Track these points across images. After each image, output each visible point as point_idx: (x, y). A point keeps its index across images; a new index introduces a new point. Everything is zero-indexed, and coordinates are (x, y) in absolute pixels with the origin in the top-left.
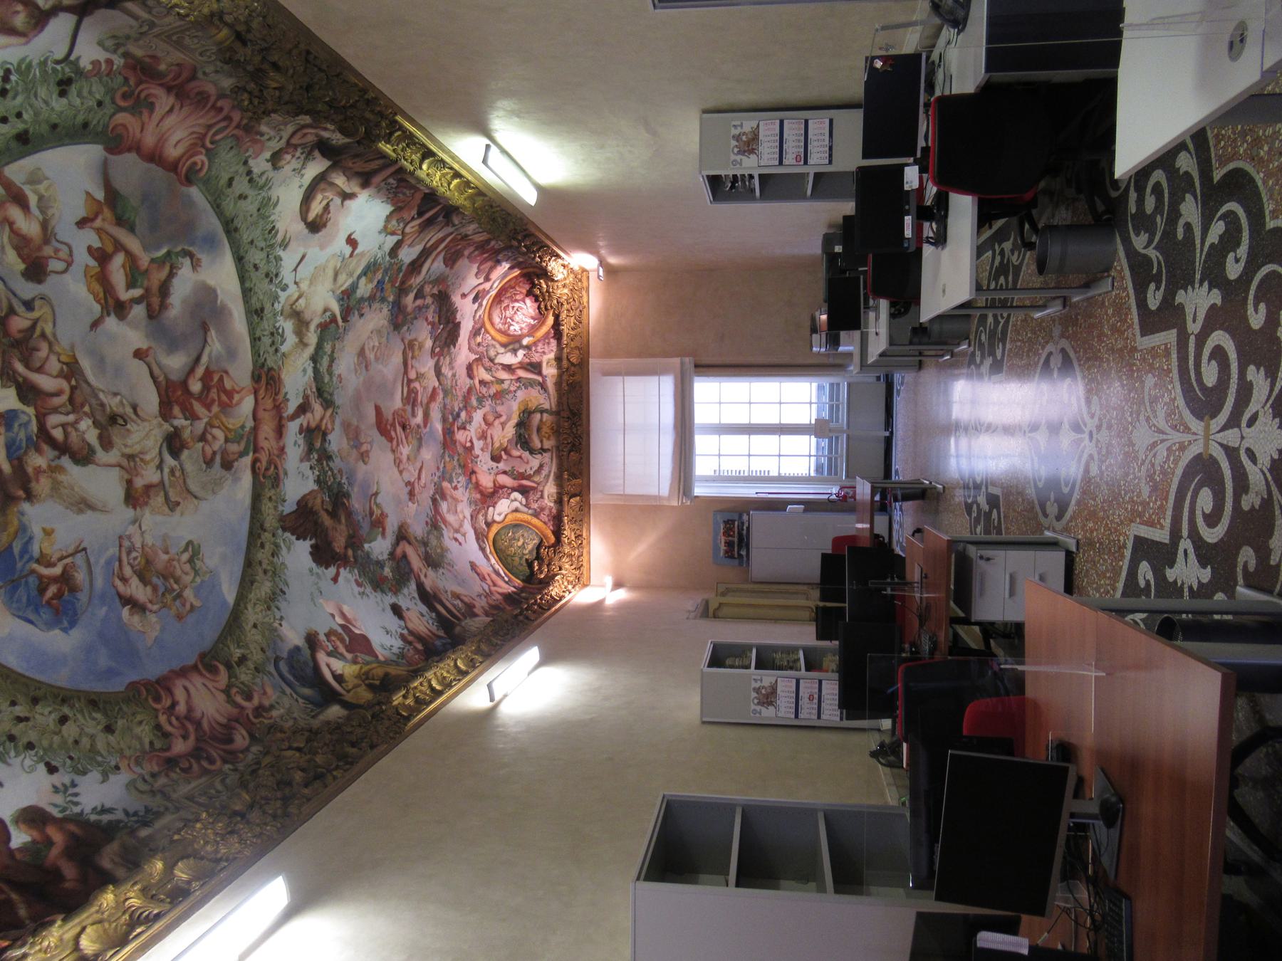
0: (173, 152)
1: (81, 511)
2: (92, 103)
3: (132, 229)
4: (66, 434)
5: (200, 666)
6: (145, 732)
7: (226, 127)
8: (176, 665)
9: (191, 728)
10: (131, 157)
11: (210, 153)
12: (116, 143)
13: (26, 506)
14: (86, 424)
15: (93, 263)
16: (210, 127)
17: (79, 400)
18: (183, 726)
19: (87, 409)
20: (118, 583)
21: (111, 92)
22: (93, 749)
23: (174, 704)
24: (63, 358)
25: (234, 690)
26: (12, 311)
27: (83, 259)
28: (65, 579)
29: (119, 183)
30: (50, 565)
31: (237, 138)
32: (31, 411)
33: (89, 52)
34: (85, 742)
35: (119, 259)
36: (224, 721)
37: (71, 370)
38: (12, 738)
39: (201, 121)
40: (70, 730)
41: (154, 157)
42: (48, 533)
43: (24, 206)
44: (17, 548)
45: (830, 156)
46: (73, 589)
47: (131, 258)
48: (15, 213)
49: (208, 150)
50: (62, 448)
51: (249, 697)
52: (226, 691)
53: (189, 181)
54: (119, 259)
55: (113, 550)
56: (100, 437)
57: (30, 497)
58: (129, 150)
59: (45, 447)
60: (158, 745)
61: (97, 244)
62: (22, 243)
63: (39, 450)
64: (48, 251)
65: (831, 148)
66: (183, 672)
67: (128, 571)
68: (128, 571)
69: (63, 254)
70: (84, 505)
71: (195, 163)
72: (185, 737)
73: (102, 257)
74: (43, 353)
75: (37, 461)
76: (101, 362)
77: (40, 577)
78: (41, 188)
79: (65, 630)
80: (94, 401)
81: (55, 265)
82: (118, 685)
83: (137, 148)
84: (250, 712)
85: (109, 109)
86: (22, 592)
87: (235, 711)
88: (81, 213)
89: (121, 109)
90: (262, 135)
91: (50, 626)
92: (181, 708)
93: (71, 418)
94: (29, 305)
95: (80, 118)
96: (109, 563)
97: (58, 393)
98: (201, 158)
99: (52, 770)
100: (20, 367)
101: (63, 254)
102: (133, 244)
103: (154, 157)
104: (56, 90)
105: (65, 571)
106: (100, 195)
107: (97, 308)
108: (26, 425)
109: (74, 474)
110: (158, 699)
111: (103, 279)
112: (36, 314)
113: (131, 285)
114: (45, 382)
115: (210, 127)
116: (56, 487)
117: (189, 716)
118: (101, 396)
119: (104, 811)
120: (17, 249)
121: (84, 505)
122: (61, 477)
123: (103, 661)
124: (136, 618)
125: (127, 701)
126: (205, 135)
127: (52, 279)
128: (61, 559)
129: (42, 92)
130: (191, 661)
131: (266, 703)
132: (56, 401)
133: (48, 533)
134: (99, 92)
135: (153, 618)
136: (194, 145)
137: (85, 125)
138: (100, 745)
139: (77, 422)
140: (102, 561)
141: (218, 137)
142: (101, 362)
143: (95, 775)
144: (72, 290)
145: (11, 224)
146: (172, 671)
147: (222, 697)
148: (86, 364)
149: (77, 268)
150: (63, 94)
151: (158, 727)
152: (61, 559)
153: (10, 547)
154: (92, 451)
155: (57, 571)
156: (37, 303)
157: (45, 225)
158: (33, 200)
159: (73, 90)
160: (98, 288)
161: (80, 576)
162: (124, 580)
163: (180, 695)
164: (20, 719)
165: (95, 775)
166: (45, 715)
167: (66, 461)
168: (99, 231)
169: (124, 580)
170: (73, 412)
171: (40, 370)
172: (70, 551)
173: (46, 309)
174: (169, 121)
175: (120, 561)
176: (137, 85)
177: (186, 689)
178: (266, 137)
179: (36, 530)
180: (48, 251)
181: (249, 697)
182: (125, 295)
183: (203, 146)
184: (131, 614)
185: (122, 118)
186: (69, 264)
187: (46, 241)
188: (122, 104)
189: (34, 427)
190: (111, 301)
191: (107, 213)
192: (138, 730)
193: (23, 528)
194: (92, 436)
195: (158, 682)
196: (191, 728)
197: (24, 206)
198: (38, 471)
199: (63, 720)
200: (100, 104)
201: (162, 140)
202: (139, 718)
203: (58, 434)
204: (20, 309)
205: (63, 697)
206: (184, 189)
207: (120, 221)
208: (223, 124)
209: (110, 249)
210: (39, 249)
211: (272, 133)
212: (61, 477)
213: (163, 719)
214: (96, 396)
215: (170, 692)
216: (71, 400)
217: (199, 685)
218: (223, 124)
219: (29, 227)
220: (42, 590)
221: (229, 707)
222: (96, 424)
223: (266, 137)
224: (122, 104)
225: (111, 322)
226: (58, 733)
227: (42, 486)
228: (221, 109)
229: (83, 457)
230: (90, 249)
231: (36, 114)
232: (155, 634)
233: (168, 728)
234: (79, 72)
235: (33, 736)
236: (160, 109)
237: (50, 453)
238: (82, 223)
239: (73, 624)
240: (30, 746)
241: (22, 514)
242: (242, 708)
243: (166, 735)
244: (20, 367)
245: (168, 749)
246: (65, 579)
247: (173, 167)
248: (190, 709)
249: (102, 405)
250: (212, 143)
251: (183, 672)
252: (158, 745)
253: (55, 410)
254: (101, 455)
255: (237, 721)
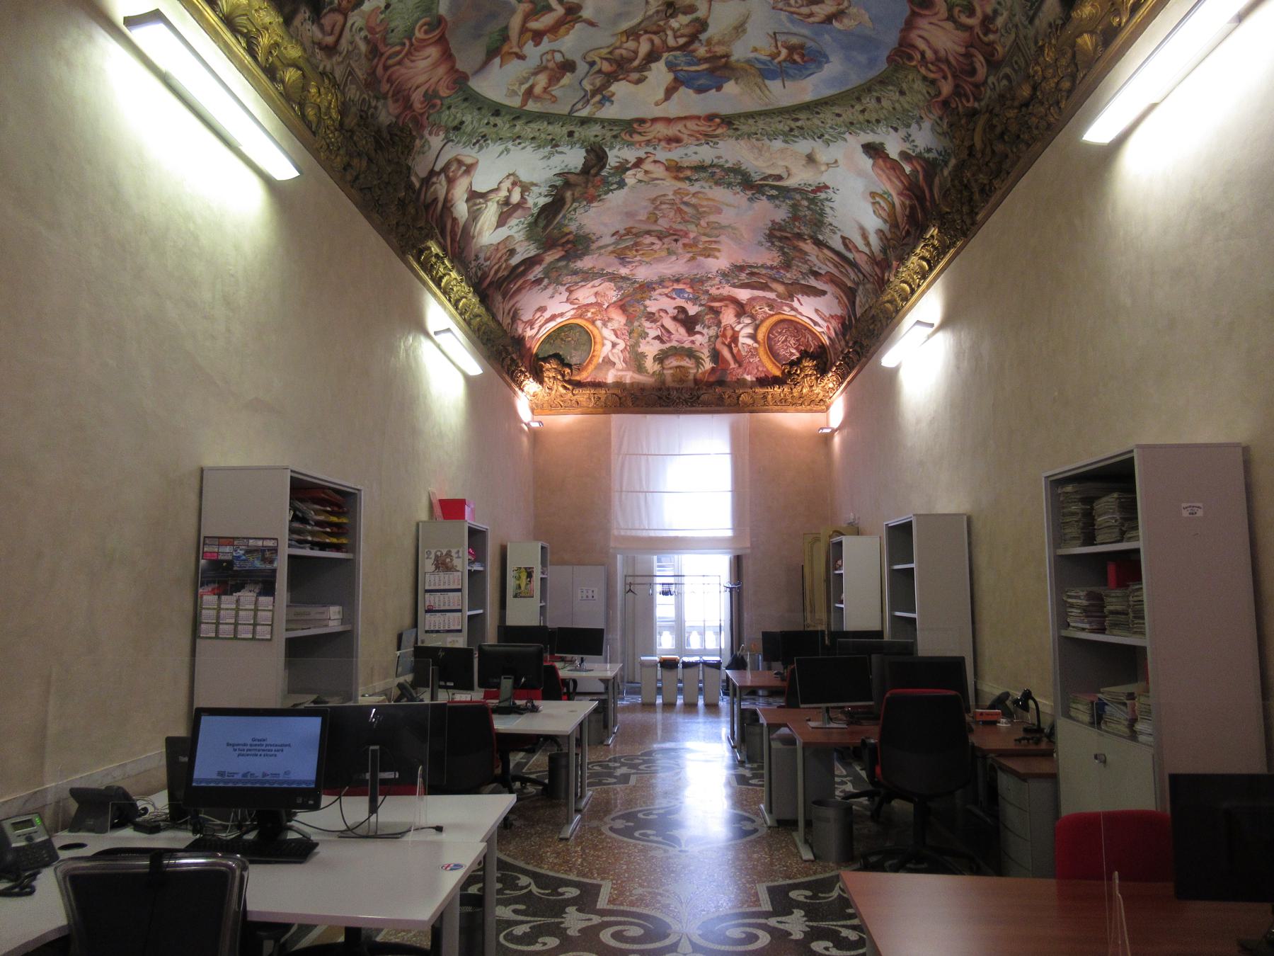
0: (433, 52)
1: (744, 31)
2: (453, 110)
3: (506, 28)
4: (682, 36)
5: (916, 10)
6: (919, 85)
7: (389, 58)
8: (900, 24)
9: (944, 67)
10: (459, 66)
11: (410, 34)
12: (460, 81)
13: (733, 59)
14: (674, 23)
15: (545, 39)
16: (400, 63)
17: (655, 28)
18: (943, 70)
19: (662, 23)
20: (811, 20)
21: (439, 112)
22: (904, 110)
23: (923, 54)
24: (624, 39)
25: (956, 10)
26: (600, 71)
27: (546, 45)
28: (791, 49)
29: (481, 57)
30: (779, 53)
31: (384, 39)
32: (665, 55)
33: (436, 141)
34: (897, 105)
35: (534, 25)
36: (962, 50)
37: (633, 34)
38: (868, 121)
39: (403, 71)
40: (885, 103)
41: (447, 56)
42: (755, 50)
43: (532, 87)
44: (759, 66)
45: (432, 632)
46: (802, 47)
47: (527, 17)
48: (538, 90)
49: (410, 39)
50: (693, 38)
51: (971, 12)
52: (951, 18)
53: (440, 21)
54: (534, 25)
55: (783, 16)
56: (685, 13)
57: (727, 56)
58: (457, 71)
59: (692, 47)
60: (933, 93)
61: (531, 43)
62: (554, 79)
63: (694, 51)
64: (551, 65)
65: (438, 631)
66: (909, 25)
67: (805, 10)
68: (805, 10)
69: (549, 57)
70: (740, 29)
71: (426, 32)
72: (945, 78)
73: (538, 36)
74: (624, 52)
75: (702, 51)
76: (620, 16)
77: (785, 60)
78: (515, 88)
79: (828, 61)
80: (655, 18)
81: (559, 58)
82: (882, 66)
83: (453, 69)
84: (978, 30)
85: (447, 102)
86: (791, 72)
87: (965, 35)
88: (516, 62)
89: (442, 99)
90: (366, 37)
91: (820, 66)
92: (929, 55)
93: (670, 33)
94: (592, 64)
95: (466, 104)
96: (792, 21)
97: (652, 41)
98: (419, 34)
99: (896, 130)
100: (636, 63)
101: (549, 57)
102: (516, 22)
103: (447, 56)
104: (463, 127)
105: (786, 48)
106: (497, 60)
107: (578, 26)
108: (675, 57)
109: (712, 31)
110: (911, 58)
111: (554, 29)
112: (597, 59)
113: (549, 9)
114: (644, 48)
115: (400, 63)
116: (720, 43)
117: (938, 59)
118: (650, 13)
119: (929, 150)
120: (558, 80)
121: (740, 29)
122: (716, 39)
123: (862, 58)
124: (846, 21)
125: (896, 71)
126: (406, 55)
127: (569, 56)
128: (777, 47)
129: (470, 127)
130: (908, 12)
131: (989, 10)
132: (657, 40)
133: (755, 50)
134: (445, 115)
135: (853, 10)
136: (416, 50)
137: (466, 100)
138: (906, 106)
139: (673, 29)
140: (789, 25)
141: (398, 48)
142: (620, 16)
143: (914, 126)
144: (570, 43)
145: (545, 89)
146: (902, 30)
147: (949, 25)
148: (625, 25)
149: (555, 46)
150: (462, 123)
151: (925, 78)
152: (777, 47)
153: (760, 70)
154: (697, 19)
155: (784, 52)
156: (589, 59)
157: (536, 74)
158: (526, 86)
159: (456, 123)
160: (563, 30)
161: (794, 40)
162: (811, 15)
163: (921, 45)
164: (863, 111)
165: (914, 126)
166: (869, 102)
167: (703, 37)
168: (521, 47)
169: (811, 15)
170: (664, 31)
171: (636, 52)
172: (773, 42)
173: (591, 54)
174: (421, 79)
175: (793, 13)
176: (422, 114)
177: (920, 37)
178: (363, 34)
179: (752, 55)
180: (551, 65)
181: (971, 12)
182: (560, 11)
183: (412, 45)
184: (841, 22)
185: (444, 92)
186: (554, 51)
187: (546, 68)
188: (438, 102)
189: (678, 53)
190: (569, 18)
191: (505, 48)
192: (915, 86)
193: (748, 61)
194: (684, 19)
195: (901, 45)
196: (944, 67)
197: (532, 87)
198: (709, 51)
199: (878, 100)
200: (449, 108)
201: (435, 65)
202: (910, 77)
203: (682, 41)
204: (596, 68)
205: (867, 88)
206: (448, 19)
207: (505, 38)
208: (391, 62)
209: (529, 35)
210: (552, 70)
211: (357, 39)
212: (716, 39)
213: (923, 70)
214: (651, 17)
215: (914, 47)
216: (655, 33)
217: (927, 27)
218: (391, 62)
219: (542, 80)
220: (795, 62)
221: (959, 33)
222: (672, 16)
223: (363, 34)
224: (438, 102)
225: (586, 13)
226: (882, 108)
227: (720, 50)
228: (388, 81)
229: (702, 25)
230: (537, 45)
231: (480, 120)
232: (867, 17)
233: (932, 76)
234: (447, 132)
235: (874, 117)
236: (422, 90)
237: (696, 45)
238: (522, 57)
239: (826, 56)
240: (878, 121)
241: (738, 61)
242: (970, 28)
243: (933, 82)
244: (636, 63)
245: (940, 93)
246: (791, 49)
247: (442, 41)
248: (936, 52)
249: (657, 12)
250: (404, 44)
251: (909, 25)
252: (933, 93)
253: (664, 42)
254: (701, 13)
255: (972, 46)
